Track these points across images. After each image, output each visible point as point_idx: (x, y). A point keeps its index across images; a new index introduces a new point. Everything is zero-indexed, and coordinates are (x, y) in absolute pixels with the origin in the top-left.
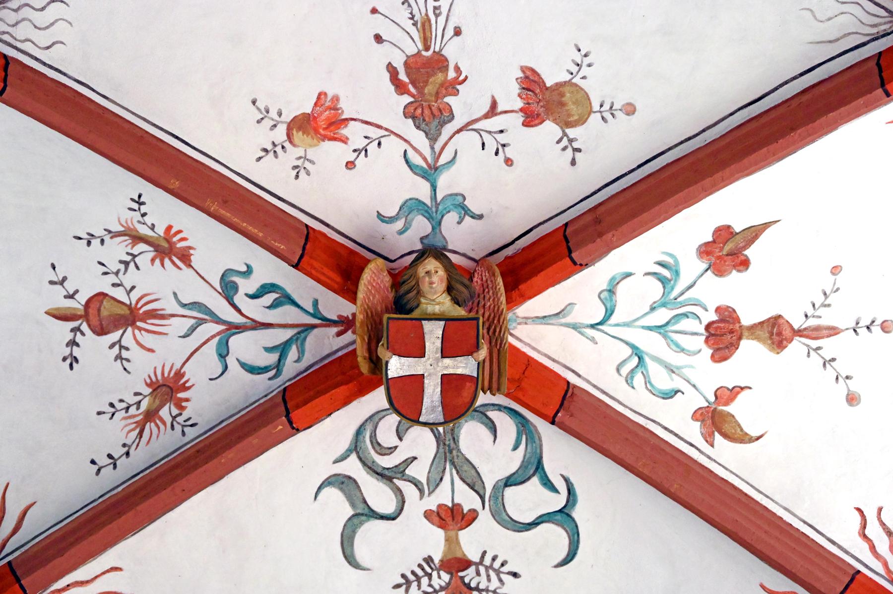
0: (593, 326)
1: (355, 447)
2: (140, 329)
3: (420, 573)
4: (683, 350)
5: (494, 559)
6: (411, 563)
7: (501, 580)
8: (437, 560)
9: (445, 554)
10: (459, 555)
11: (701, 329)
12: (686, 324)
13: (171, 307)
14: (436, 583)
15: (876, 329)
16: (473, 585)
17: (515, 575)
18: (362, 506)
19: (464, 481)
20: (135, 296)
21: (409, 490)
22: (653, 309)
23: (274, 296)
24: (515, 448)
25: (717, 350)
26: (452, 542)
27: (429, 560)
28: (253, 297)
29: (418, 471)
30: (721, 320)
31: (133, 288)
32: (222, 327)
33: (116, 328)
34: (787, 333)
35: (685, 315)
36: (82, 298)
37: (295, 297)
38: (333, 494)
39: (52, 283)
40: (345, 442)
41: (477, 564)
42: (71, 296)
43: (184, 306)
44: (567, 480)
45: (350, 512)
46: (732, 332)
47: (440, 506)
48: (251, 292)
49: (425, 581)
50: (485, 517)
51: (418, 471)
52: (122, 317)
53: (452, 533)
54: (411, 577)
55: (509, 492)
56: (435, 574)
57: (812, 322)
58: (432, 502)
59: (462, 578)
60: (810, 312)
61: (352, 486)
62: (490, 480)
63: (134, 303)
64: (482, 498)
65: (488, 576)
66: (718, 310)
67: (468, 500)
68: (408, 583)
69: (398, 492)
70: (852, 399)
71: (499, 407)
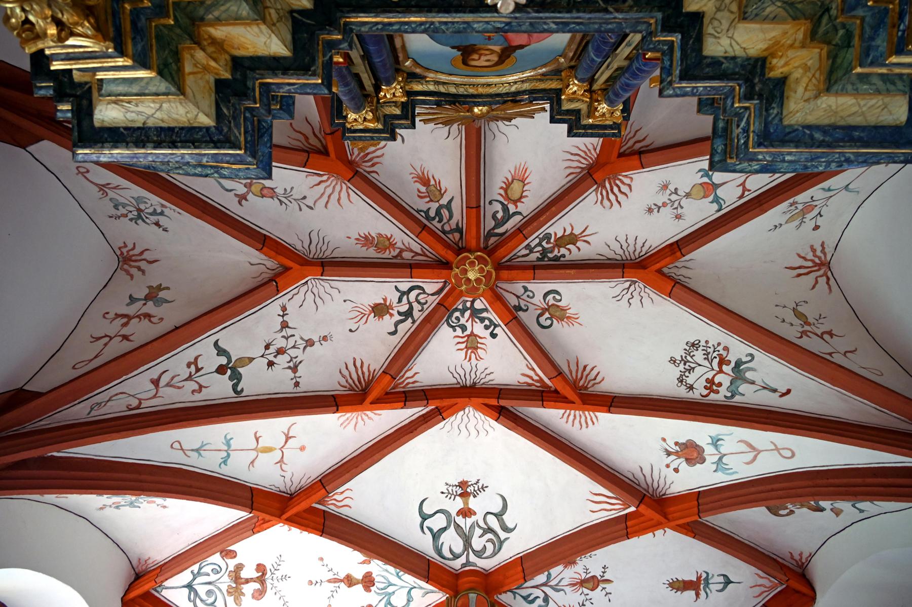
0: (415, 587)
1: (501, 543)
2: (579, 579)
3: (478, 492)
4: (383, 576)
5: (450, 498)
6: (482, 495)
7: (448, 490)
8: (472, 496)
9: (469, 499)
10: (463, 498)
11: (376, 584)
12: (382, 586)
13: (568, 589)
14: (472, 488)
15: (314, 582)
16: (458, 487)
17: (442, 493)
18: (499, 519)
19: (462, 528)
20: (580, 591)
21: (482, 524)
22: (394, 592)
23: (530, 598)
24: (443, 543)
25: (371, 576)
26: (466, 503)
27: (475, 496)
28: (538, 597)
29: (478, 532)
30: (369, 587)
31: (581, 594)
32: (549, 584)
33: (588, 578)
34: (346, 581)
35: (382, 589)
36: (600, 588)
37: (522, 599)
38: (510, 525)
39: (610, 593)
40: (505, 545)
41: (457, 495)
42: (604, 588)
43: (563, 590)
44: (423, 532)
45: (503, 517)
46: (365, 582)
47: (471, 517)
48: (538, 599)
49: (476, 489)
50: (454, 514)
51: (478, 532)
52: (586, 583)
53: (466, 506)
54: (481, 490)
55: (444, 525)
56: (472, 491)
57: (337, 585)
58: (474, 518)
59: (462, 490)
60: (338, 589)
61: (503, 527)
62: (452, 529)
63: (581, 589)
64: (455, 521)
65: (452, 490)
66: (370, 591)
67: (460, 520)
68: (482, 488)
69: (486, 523)
70: (321, 559)
71: (449, 559)
